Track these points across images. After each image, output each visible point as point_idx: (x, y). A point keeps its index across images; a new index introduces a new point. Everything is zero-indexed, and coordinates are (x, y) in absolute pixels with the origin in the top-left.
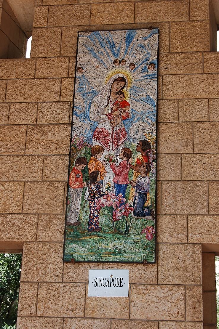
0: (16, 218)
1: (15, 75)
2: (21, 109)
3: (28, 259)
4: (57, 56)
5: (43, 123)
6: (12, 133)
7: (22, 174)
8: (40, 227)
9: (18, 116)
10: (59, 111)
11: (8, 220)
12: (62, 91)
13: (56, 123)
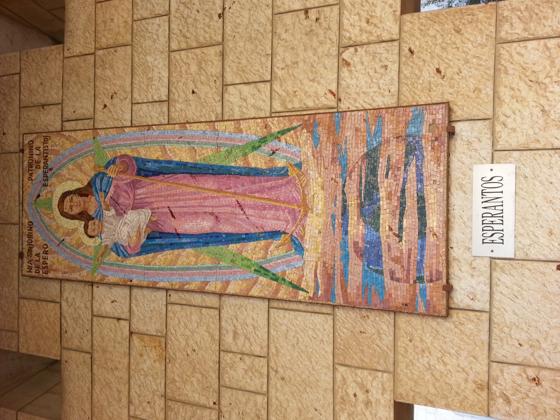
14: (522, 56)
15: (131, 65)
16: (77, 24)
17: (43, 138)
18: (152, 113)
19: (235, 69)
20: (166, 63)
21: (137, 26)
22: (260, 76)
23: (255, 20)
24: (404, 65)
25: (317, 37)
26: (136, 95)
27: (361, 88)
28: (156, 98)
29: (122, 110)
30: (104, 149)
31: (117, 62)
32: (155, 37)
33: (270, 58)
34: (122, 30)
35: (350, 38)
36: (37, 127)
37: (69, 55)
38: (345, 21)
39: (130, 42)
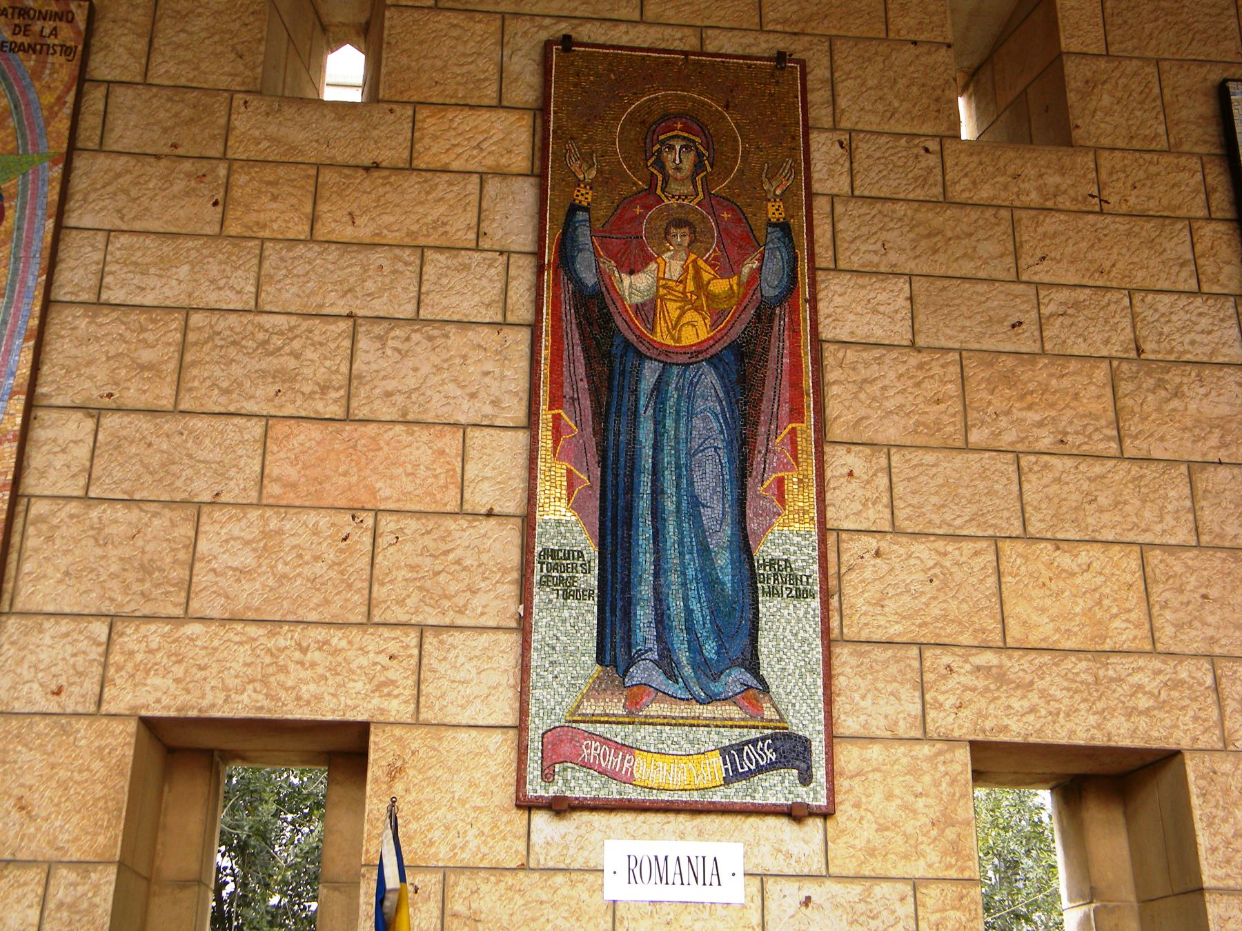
0: (1140, 669)
1: (1034, 195)
2: (1076, 305)
3: (1214, 810)
4: (1158, 148)
5: (1160, 357)
6: (1066, 382)
7: (1129, 519)
8: (1229, 701)
9: (1074, 328)
10: (1204, 323)
11: (1111, 673)
12: (1200, 262)
13: (1205, 359)
14: (19, 901)
15: (184, 231)
16: (290, 124)
17: (73, 44)
18: (81, 271)
19: (125, 433)
20: (168, 303)
21: (251, 248)
22: (99, 479)
23: (198, 472)
24: (55, 722)
25: (138, 580)
26: (124, 240)
27: (32, 652)
28: (108, 279)
29: (102, 209)
30: (24, 175)
31: (194, 205)
32: (222, 283)
33: (126, 497)
34: (253, 217)
35: (122, 634)
36: (110, 25)
37: (235, 104)
38: (153, 627)
39: (225, 233)
